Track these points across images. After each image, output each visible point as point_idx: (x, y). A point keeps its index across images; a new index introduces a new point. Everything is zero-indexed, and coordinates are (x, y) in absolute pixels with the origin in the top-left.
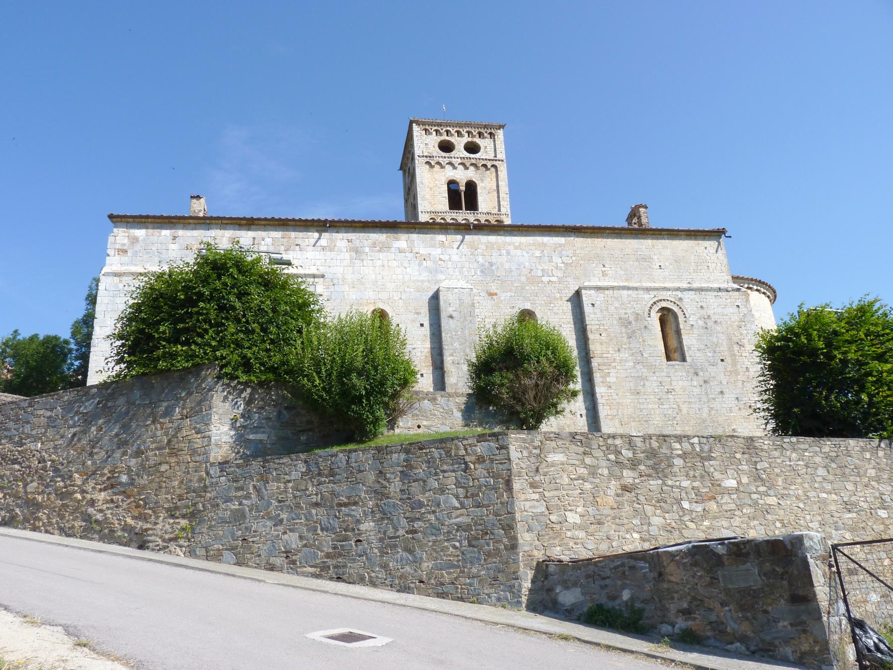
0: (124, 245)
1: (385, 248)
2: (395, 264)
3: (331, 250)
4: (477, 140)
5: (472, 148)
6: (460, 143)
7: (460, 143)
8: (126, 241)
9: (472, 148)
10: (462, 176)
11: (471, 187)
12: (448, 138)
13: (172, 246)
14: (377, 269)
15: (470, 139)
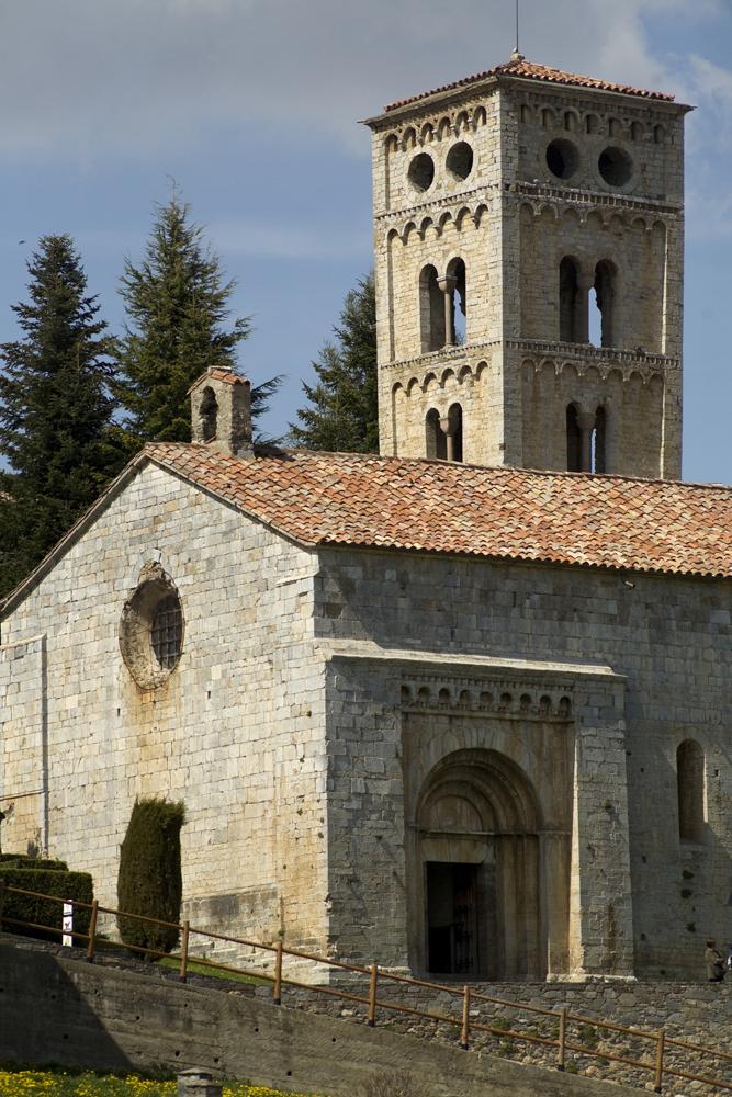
0: (335, 595)
1: (697, 621)
2: (712, 655)
3: (623, 623)
4: (628, 147)
5: (612, 166)
6: (590, 147)
7: (590, 147)
8: (336, 589)
9: (612, 166)
10: (587, 246)
11: (605, 275)
12: (566, 135)
13: (403, 603)
14: (688, 662)
15: (612, 142)
